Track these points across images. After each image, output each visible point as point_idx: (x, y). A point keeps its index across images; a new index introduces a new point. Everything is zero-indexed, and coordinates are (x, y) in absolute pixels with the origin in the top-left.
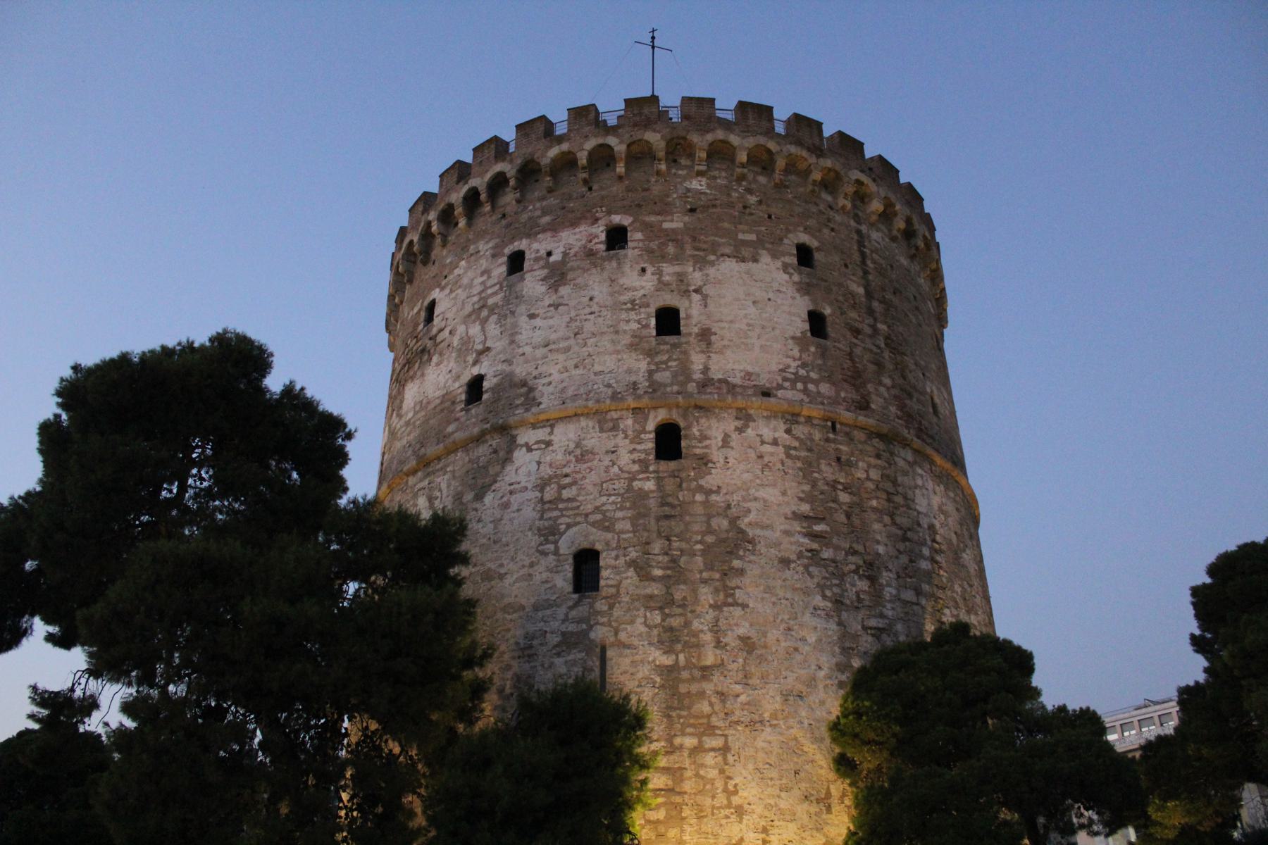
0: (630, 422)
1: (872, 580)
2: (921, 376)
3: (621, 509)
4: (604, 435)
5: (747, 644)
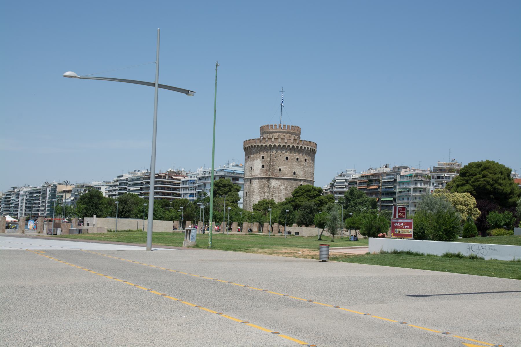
1: (264, 194)
5: (254, 201)
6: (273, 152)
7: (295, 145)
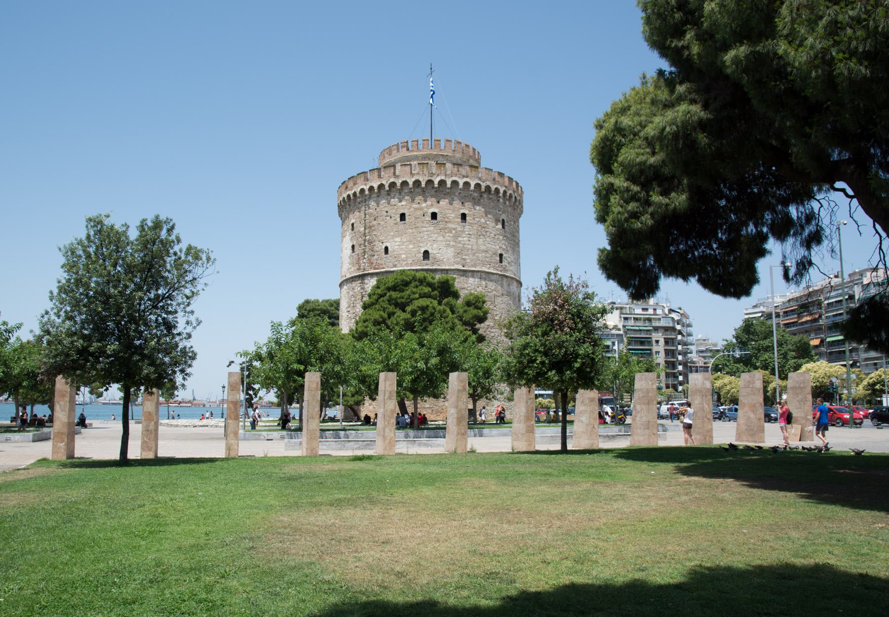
2: (381, 244)
6: (369, 208)
7: (421, 179)
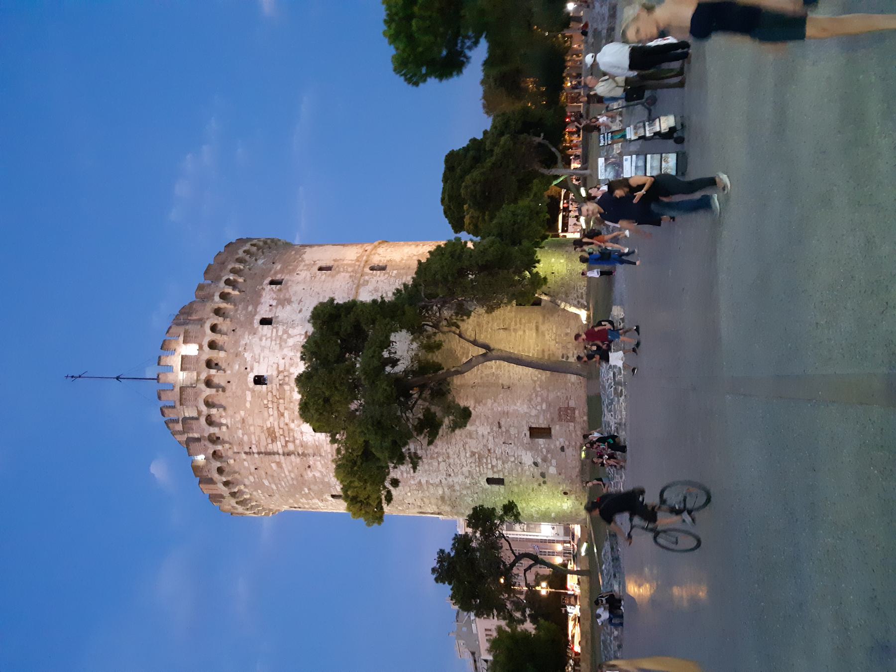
0: (366, 277)
3: (402, 279)
4: (369, 284)
